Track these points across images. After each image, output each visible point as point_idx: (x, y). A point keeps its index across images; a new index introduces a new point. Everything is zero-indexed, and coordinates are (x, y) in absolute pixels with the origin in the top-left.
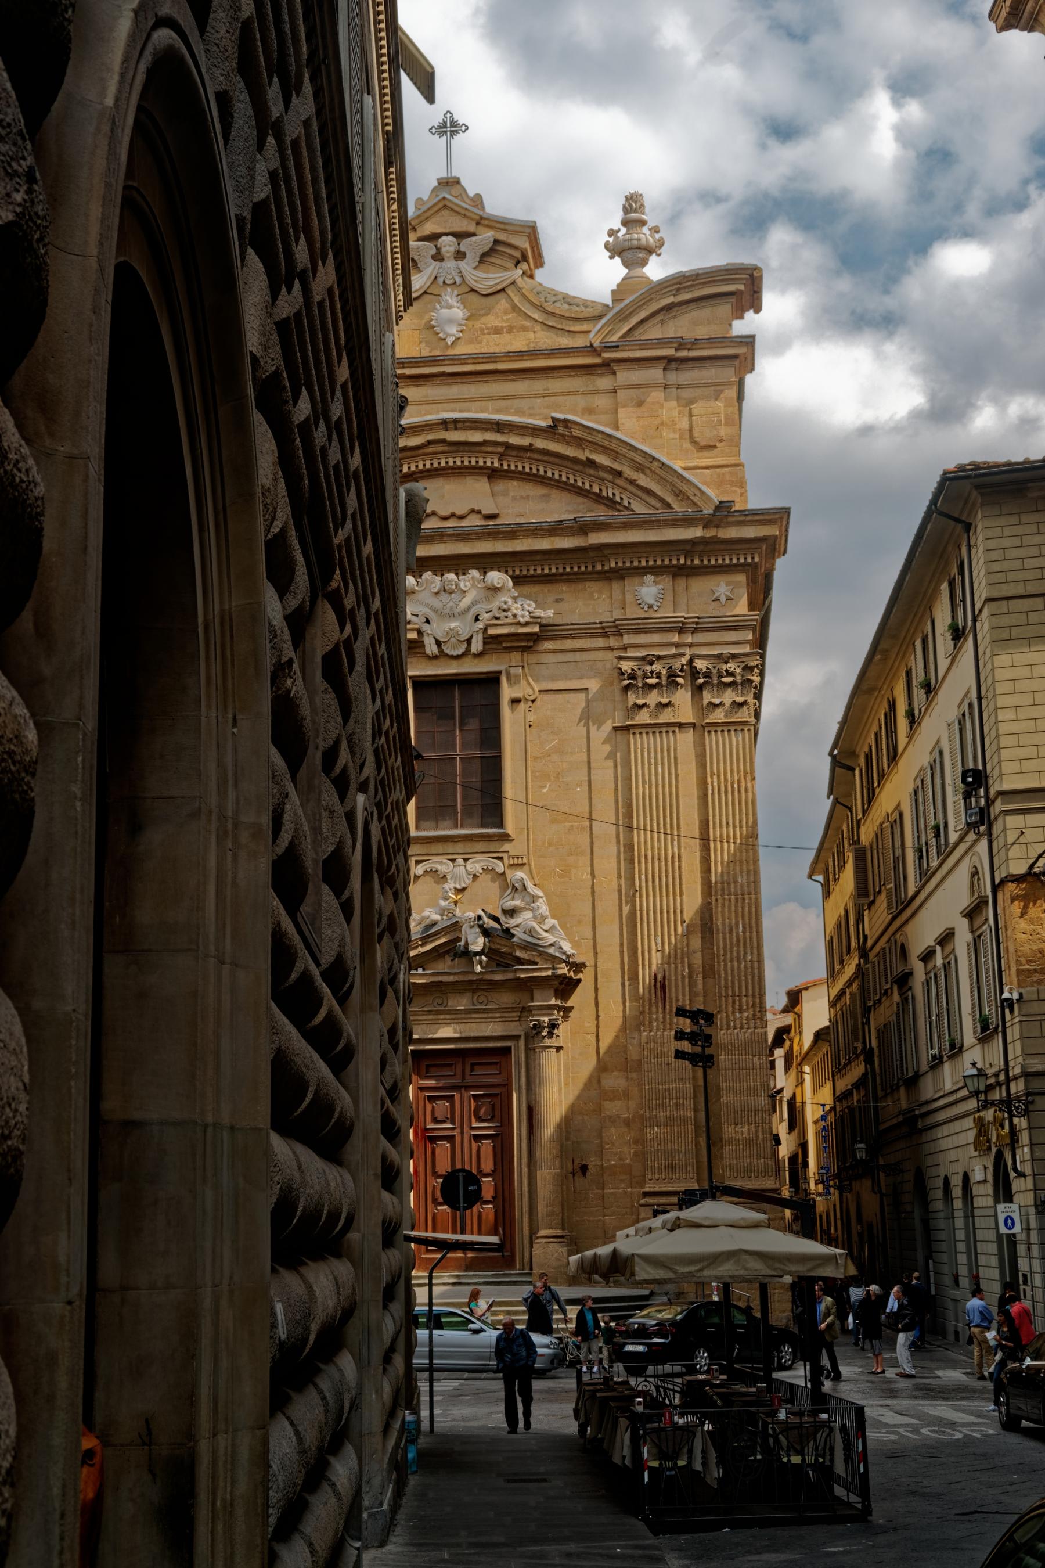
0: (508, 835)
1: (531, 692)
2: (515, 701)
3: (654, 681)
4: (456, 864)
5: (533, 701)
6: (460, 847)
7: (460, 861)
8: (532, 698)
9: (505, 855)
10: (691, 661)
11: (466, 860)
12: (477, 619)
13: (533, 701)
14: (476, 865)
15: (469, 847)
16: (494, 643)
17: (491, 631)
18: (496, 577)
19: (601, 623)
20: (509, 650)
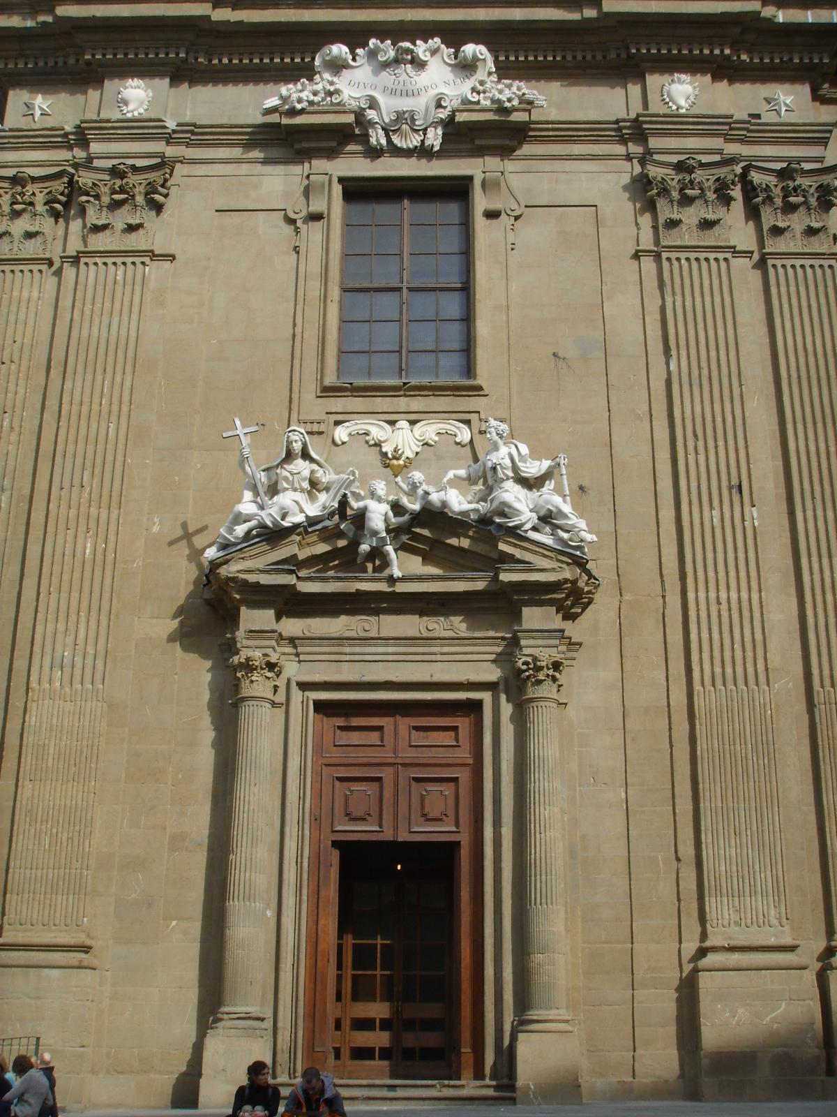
0: (480, 388)
1: (515, 206)
2: (492, 215)
3: (696, 192)
4: (398, 425)
5: (517, 218)
6: (403, 403)
7: (403, 424)
8: (516, 213)
9: (474, 417)
10: (746, 170)
11: (413, 423)
12: (439, 105)
13: (517, 218)
14: (429, 430)
15: (417, 404)
16: (463, 135)
17: (460, 118)
18: (470, 49)
19: (617, 122)
20: (480, 152)
